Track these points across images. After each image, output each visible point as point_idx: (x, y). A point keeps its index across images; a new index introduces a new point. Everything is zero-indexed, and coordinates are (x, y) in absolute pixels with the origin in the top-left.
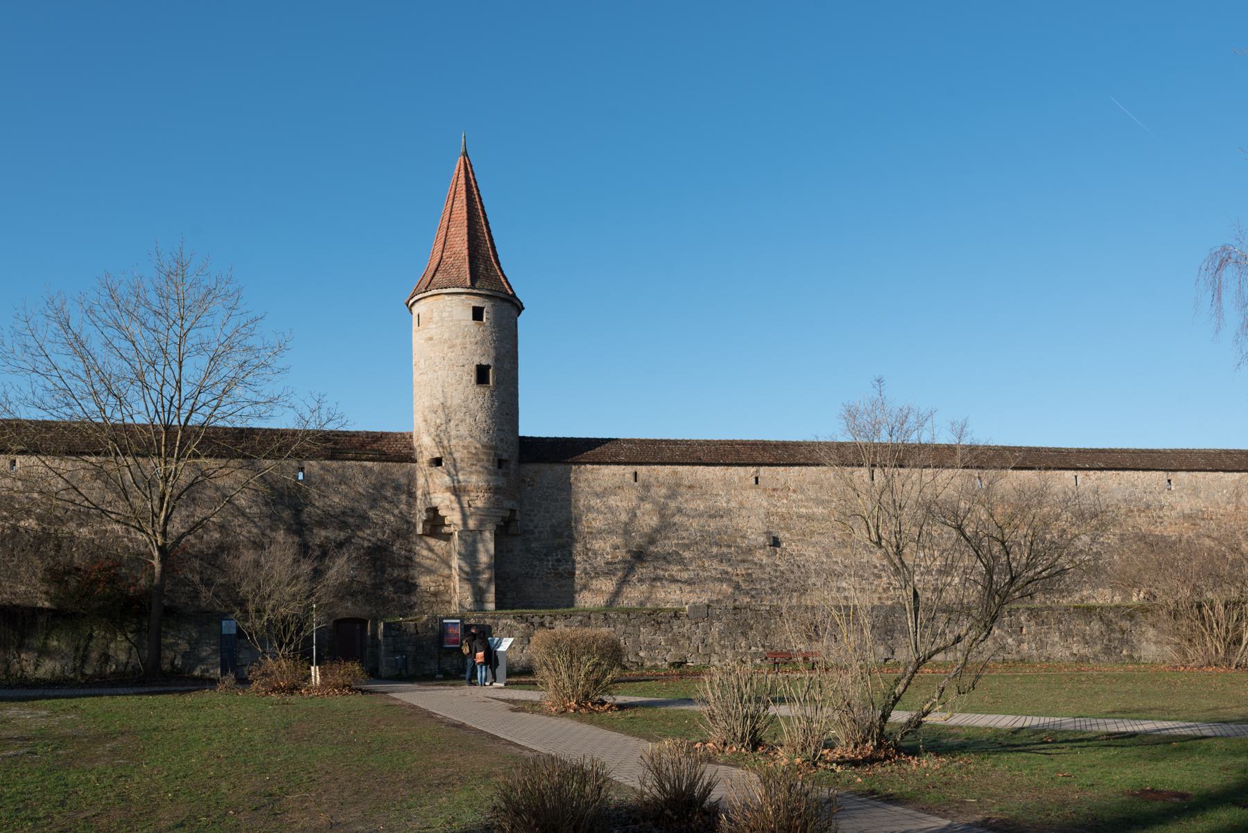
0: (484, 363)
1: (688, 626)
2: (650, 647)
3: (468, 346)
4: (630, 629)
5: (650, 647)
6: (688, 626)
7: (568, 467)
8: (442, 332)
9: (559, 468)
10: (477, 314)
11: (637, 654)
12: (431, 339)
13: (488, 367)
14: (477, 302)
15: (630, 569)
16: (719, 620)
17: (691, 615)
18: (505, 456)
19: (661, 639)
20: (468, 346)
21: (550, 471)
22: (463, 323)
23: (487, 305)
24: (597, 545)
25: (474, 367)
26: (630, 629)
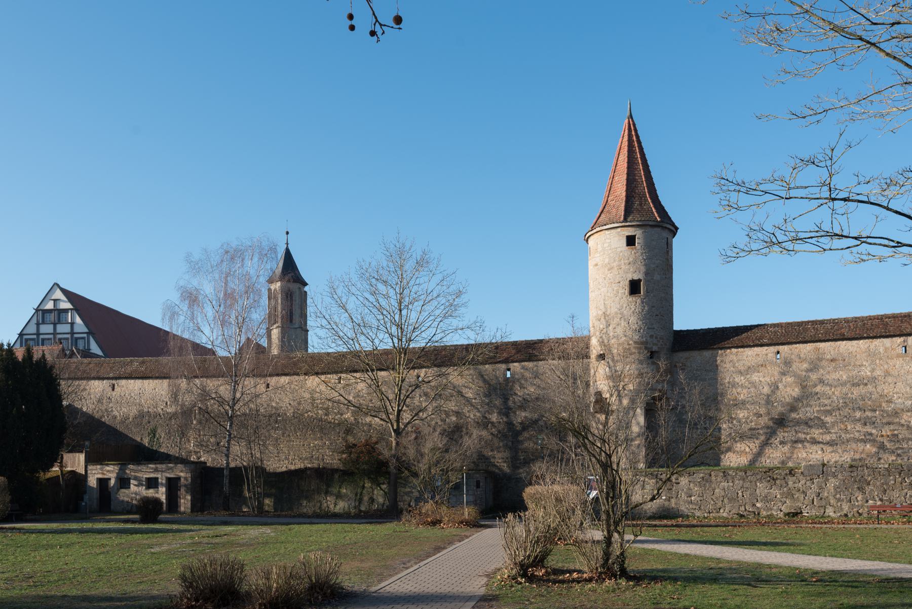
0: (636, 278)
1: (803, 482)
2: (766, 499)
3: (623, 267)
4: (747, 485)
5: (766, 499)
6: (803, 482)
7: (715, 352)
8: (608, 256)
9: (707, 354)
10: (631, 241)
11: (754, 505)
12: (596, 265)
13: (640, 281)
14: (630, 232)
15: (771, 433)
16: (835, 476)
17: (806, 472)
18: (655, 348)
19: (776, 492)
20: (623, 267)
21: (699, 357)
22: (619, 250)
23: (638, 233)
24: (741, 414)
25: (627, 283)
26: (747, 485)
